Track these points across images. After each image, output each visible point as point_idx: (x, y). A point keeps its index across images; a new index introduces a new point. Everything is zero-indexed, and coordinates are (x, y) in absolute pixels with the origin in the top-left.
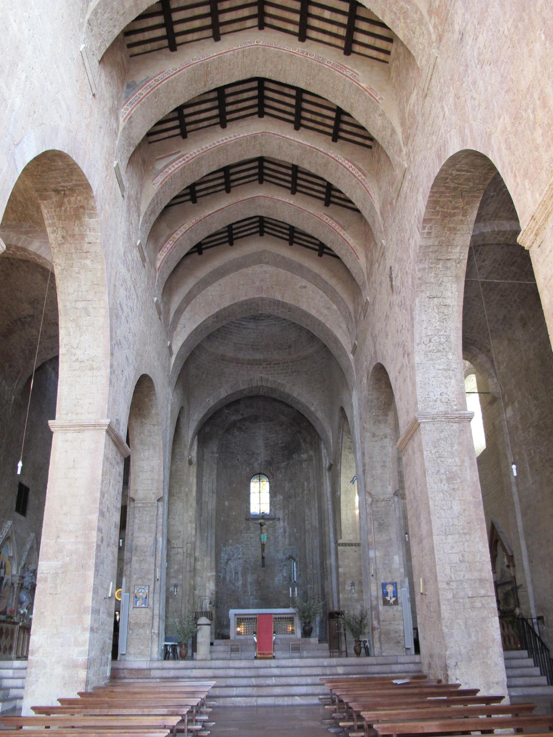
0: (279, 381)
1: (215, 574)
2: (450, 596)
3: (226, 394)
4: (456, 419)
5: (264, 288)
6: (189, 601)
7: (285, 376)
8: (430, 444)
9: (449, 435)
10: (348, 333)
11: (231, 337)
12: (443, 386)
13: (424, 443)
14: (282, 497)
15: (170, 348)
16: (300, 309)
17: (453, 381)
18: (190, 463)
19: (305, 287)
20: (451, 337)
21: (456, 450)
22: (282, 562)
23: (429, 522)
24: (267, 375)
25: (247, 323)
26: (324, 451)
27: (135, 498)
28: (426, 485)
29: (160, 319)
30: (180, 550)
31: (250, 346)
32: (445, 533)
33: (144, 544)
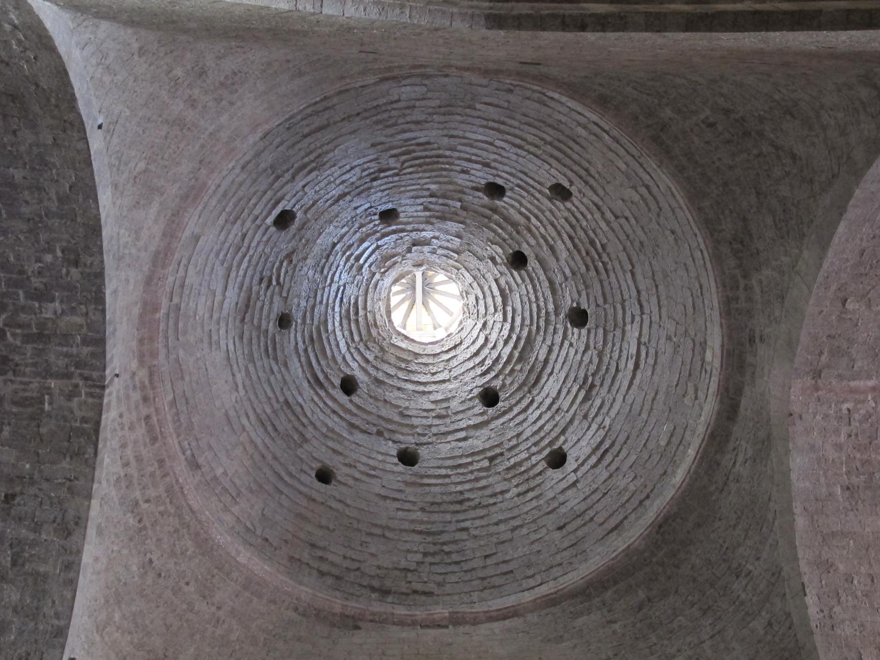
7: (118, 480)
11: (221, 221)
25: (239, 279)
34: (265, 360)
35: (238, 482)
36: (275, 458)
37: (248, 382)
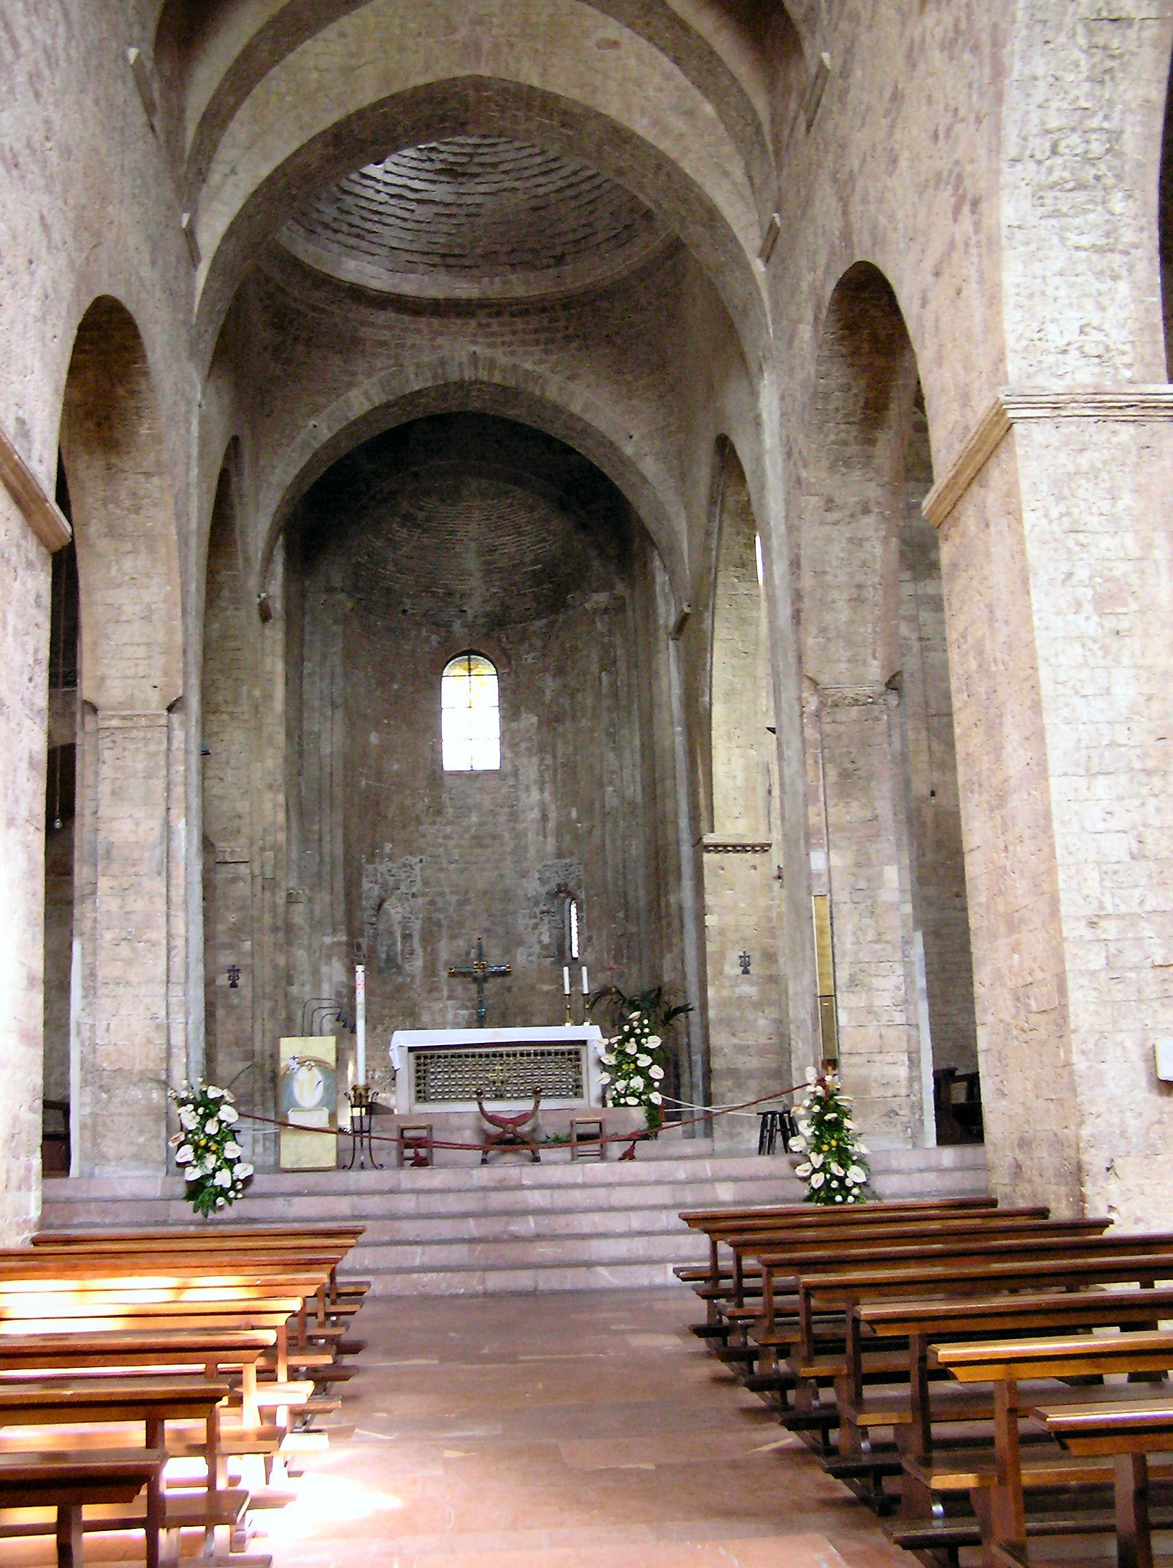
0: (528, 366)
1: (344, 938)
2: (1096, 961)
3: (367, 407)
4: (1130, 411)
5: (486, 46)
6: (273, 1012)
7: (546, 352)
8: (1044, 488)
9: (1105, 462)
10: (747, 192)
12: (1089, 304)
13: (1024, 484)
14: (534, 719)
15: (190, 234)
16: (598, 115)
17: (1123, 287)
18: (265, 615)
19: (615, 44)
20: (1125, 136)
21: (1128, 509)
22: (537, 904)
23: (1037, 736)
24: (492, 345)
26: (661, 579)
27: (99, 701)
28: (1027, 619)
29: (152, 127)
30: (243, 870)
31: (437, 260)
32: (1087, 770)
33: (132, 838)
34: (500, 148)
35: (583, 222)
36: (575, 173)
37: (515, 175)
